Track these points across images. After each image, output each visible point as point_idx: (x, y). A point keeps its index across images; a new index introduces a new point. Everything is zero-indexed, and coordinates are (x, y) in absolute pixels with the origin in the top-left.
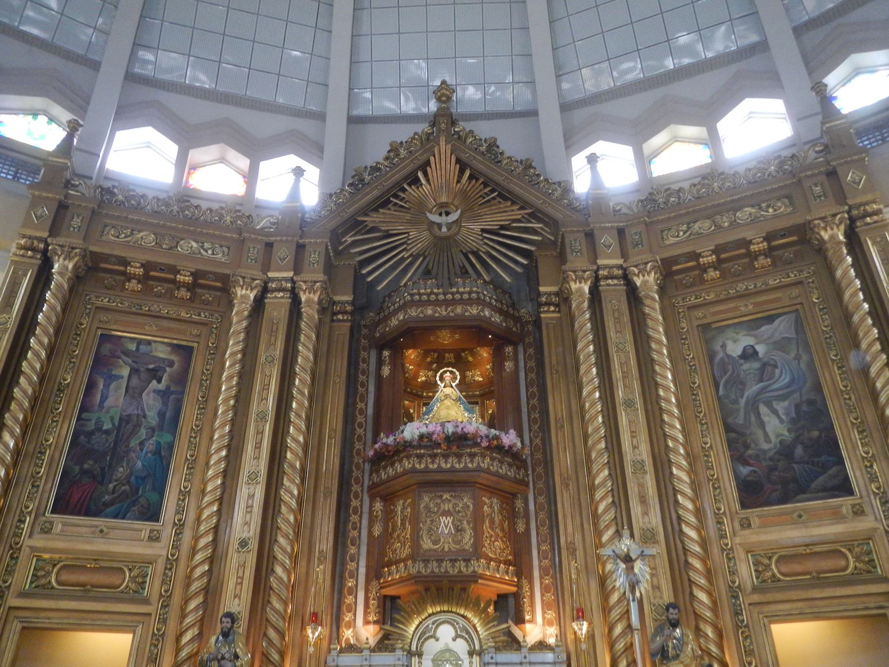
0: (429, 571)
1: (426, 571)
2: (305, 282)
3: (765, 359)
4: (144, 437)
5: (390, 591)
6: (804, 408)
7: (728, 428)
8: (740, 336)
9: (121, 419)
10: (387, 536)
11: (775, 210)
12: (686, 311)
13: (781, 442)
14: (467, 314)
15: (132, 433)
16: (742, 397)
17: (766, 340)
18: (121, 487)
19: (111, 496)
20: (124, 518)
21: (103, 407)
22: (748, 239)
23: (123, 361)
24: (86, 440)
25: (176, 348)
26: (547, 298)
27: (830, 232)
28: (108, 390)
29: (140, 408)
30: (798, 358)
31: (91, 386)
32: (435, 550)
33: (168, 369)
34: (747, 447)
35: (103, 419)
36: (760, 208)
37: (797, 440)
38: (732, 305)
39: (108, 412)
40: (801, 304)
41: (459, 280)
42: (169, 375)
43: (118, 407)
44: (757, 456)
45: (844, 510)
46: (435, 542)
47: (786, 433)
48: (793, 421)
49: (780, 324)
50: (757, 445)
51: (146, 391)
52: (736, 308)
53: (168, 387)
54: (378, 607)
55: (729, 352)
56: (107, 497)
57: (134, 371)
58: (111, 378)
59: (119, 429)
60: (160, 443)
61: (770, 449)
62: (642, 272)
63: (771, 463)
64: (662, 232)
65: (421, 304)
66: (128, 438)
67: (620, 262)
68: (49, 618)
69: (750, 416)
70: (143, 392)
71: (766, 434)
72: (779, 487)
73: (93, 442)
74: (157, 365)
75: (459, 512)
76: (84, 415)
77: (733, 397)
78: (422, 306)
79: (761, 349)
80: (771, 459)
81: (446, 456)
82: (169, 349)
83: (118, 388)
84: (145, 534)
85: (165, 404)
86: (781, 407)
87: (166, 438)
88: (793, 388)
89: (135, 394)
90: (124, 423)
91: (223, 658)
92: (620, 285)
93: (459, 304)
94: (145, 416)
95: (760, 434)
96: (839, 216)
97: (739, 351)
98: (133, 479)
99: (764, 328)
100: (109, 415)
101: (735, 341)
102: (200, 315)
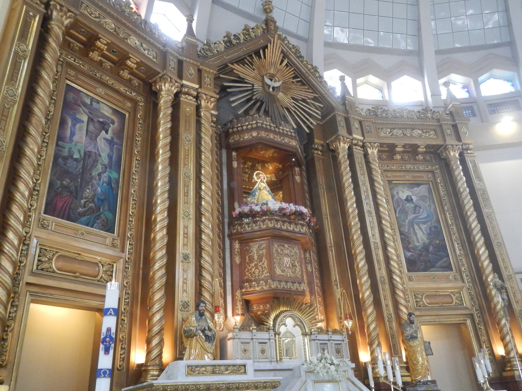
0: (282, 287)
1: (280, 287)
2: (205, 95)
3: (416, 204)
4: (100, 171)
5: (247, 297)
6: (433, 229)
7: (401, 233)
8: (405, 190)
9: (85, 153)
10: (243, 265)
11: (429, 135)
12: (383, 171)
13: (424, 243)
14: (291, 144)
15: (92, 165)
16: (407, 219)
17: (416, 194)
18: (89, 204)
19: (84, 209)
20: (92, 227)
21: (73, 141)
22: (419, 145)
23: (82, 109)
24: (63, 162)
26: (318, 146)
27: (454, 153)
28: (75, 128)
29: (96, 148)
30: (429, 206)
31: (63, 123)
32: (283, 276)
33: (111, 125)
34: (410, 243)
35: (73, 149)
36: (423, 132)
37: (430, 243)
38: (402, 174)
39: (76, 145)
40: (432, 181)
41: (283, 122)
42: (112, 130)
43: (82, 143)
44: (414, 248)
45: (451, 277)
46: (283, 271)
47: (426, 240)
48: (429, 235)
49: (422, 188)
50: (413, 243)
51: (99, 137)
52: (404, 176)
53: (112, 138)
54: (242, 306)
55: (400, 197)
56: (80, 209)
57: (90, 120)
58: (75, 121)
59: (84, 159)
60: (110, 177)
61: (419, 246)
62: (372, 147)
63: (420, 252)
64: (379, 129)
65: (266, 130)
66: (91, 168)
67: (362, 138)
68: (51, 294)
69: (410, 229)
70: (98, 137)
71: (417, 239)
72: (423, 264)
73: (69, 165)
74: (104, 120)
75: (293, 256)
76: (60, 143)
77: (403, 218)
78: (268, 132)
79: (414, 198)
80: (420, 251)
81: (290, 223)
82: (111, 111)
83: (81, 129)
84: (108, 241)
85: (111, 149)
86: (423, 227)
87: (114, 175)
88: (428, 219)
90: (87, 157)
91: (205, 329)
92: (361, 150)
93: (287, 137)
94: (100, 156)
95: (414, 238)
96: (458, 146)
97: (405, 198)
98: (96, 199)
99: (415, 189)
100: (77, 148)
101: (403, 192)
102: (131, 93)
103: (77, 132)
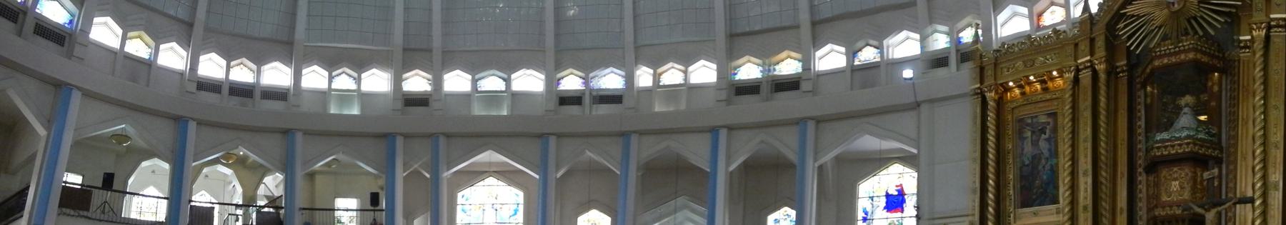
9: (1032, 158)
25: (1050, 115)
53: (1050, 135)
57: (1033, 132)
59: (1032, 162)
82: (1046, 116)
85: (1050, 144)
87: (1054, 161)
89: (1035, 143)
94: (1042, 153)
98: (1043, 185)
103: (1025, 146)
